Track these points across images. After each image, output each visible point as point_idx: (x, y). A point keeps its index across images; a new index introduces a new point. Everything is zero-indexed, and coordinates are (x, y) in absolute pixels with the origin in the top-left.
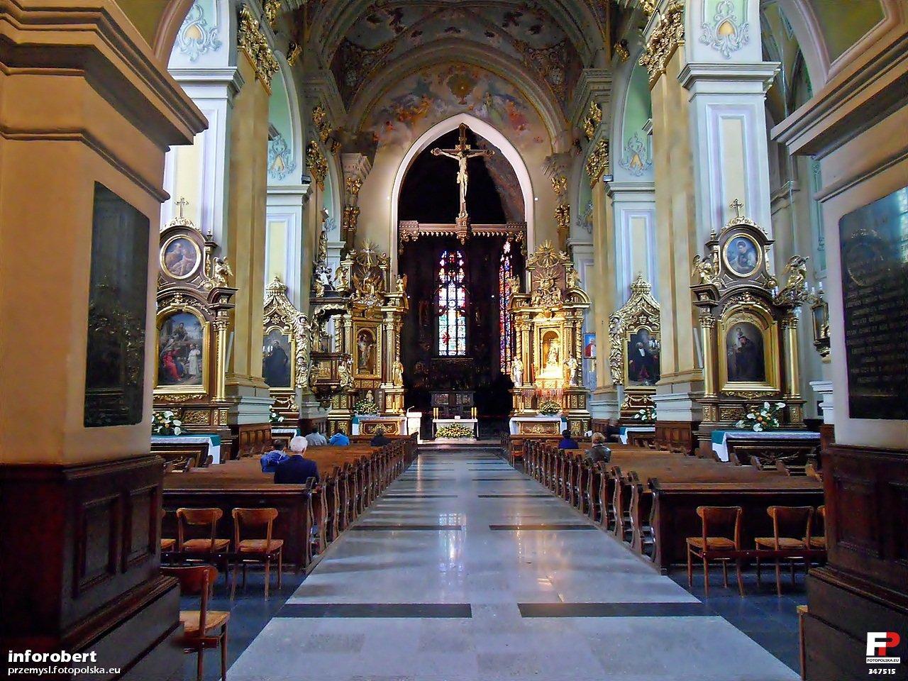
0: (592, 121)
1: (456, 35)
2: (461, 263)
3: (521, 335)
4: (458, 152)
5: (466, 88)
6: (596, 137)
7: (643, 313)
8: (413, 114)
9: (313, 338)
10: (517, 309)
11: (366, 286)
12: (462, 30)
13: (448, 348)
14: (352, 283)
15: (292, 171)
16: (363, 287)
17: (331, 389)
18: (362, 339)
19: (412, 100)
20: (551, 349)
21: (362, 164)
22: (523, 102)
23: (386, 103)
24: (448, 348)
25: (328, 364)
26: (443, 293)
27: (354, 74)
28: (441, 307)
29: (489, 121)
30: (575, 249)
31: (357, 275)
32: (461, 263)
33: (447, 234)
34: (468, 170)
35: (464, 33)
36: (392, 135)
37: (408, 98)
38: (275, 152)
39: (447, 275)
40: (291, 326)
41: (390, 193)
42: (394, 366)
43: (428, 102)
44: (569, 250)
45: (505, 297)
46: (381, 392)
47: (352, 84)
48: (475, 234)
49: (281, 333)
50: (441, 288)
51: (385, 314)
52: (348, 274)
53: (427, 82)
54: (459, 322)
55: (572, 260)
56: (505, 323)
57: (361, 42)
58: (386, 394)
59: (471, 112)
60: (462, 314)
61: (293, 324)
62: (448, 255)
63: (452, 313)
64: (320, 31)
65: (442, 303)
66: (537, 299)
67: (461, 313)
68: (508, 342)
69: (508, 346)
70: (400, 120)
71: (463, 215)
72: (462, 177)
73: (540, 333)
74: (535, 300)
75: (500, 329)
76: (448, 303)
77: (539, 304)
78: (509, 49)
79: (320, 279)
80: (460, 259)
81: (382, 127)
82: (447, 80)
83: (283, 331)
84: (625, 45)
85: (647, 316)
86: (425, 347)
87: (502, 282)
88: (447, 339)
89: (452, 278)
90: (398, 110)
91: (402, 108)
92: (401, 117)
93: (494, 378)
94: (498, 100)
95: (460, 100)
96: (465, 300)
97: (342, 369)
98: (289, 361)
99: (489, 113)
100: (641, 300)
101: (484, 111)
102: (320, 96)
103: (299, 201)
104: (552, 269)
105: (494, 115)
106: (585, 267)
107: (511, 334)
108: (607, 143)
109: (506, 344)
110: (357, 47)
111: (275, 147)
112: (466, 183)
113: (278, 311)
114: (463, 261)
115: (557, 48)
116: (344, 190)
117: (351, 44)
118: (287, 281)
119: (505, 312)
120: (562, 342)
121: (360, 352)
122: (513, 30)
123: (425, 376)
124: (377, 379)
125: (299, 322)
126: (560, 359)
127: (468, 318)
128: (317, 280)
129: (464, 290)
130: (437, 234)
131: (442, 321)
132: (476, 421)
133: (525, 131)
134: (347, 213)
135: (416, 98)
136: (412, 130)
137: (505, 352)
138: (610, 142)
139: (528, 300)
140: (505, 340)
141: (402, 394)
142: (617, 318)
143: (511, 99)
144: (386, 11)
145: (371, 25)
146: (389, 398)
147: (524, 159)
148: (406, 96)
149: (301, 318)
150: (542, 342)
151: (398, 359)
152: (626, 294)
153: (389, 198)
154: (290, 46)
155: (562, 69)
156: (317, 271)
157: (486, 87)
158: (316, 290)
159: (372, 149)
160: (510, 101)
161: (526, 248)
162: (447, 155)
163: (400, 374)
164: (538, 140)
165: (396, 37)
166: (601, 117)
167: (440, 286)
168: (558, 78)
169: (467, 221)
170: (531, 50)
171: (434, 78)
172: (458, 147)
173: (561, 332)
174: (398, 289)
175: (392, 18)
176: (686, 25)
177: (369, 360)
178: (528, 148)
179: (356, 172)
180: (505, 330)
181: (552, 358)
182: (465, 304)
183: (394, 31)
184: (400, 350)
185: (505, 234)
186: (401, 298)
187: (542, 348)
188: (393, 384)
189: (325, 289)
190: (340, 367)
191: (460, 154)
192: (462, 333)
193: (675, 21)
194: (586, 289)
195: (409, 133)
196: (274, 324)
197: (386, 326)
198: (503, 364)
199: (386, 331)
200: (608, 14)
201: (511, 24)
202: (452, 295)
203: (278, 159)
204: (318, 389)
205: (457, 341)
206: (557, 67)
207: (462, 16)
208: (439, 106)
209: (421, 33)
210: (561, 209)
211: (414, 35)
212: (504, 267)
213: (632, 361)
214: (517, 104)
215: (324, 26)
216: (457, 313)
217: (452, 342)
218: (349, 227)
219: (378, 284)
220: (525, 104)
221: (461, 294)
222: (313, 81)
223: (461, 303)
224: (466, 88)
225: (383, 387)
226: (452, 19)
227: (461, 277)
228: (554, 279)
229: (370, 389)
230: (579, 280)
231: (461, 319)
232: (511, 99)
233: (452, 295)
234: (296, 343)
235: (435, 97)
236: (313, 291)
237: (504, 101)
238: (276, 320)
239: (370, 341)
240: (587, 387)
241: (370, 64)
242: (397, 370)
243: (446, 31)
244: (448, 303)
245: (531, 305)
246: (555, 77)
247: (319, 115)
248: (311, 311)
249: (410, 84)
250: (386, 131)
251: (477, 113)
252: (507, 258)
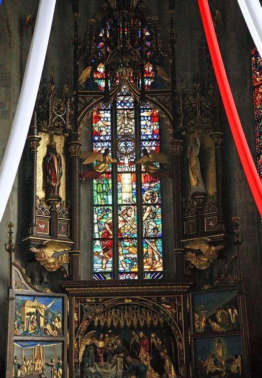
13: (116, 264)
24: (116, 264)
54: (146, 195)
60: (155, 176)
192: (154, 225)
217: (127, 252)
231: (151, 188)
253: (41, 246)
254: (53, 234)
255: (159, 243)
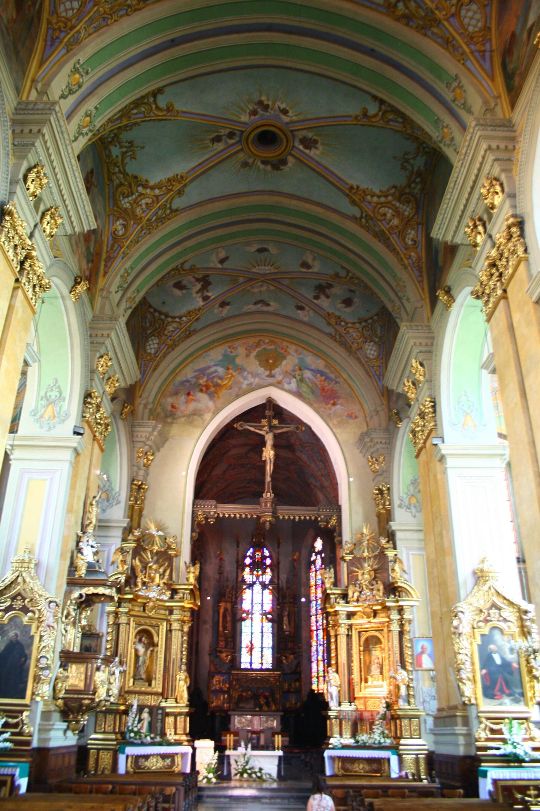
0: (414, 384)
1: (265, 309)
2: (268, 561)
3: (336, 641)
4: (264, 426)
5: (275, 361)
6: (420, 399)
7: (494, 606)
8: (217, 385)
9: (66, 631)
10: (331, 607)
11: (149, 574)
12: (271, 303)
14: (133, 569)
15: (63, 421)
16: (145, 574)
17: (81, 705)
18: (140, 641)
19: (216, 371)
20: (373, 658)
21: (155, 433)
22: (336, 377)
23: (188, 373)
25: (82, 668)
26: (247, 595)
27: (156, 341)
28: (244, 612)
29: (299, 395)
30: (399, 536)
31: (140, 561)
32: (268, 561)
33: (249, 516)
34: (275, 446)
35: (274, 306)
36: (192, 406)
37: (212, 370)
38: (47, 400)
39: (253, 574)
40: (37, 612)
41: (185, 467)
42: (178, 677)
43: (234, 374)
44: (391, 536)
45: (316, 601)
46: (160, 712)
47: (153, 351)
48: (281, 517)
49: (22, 622)
50: (245, 589)
51: (171, 611)
52: (129, 558)
53: (234, 354)
55: (395, 548)
56: (317, 630)
57: (164, 310)
58: (168, 714)
59: (279, 385)
60: (270, 620)
61: (39, 610)
62: (254, 553)
63: (257, 617)
64: (117, 281)
65: (246, 606)
66: (356, 594)
67: (267, 618)
68: (321, 654)
69: (320, 658)
70: (201, 391)
71: (268, 495)
72: (269, 453)
73: (360, 637)
74: (353, 597)
75: (311, 638)
76: (252, 607)
77: (358, 601)
78: (321, 323)
79: (82, 554)
80: (268, 557)
81: (183, 398)
82: (255, 353)
83: (25, 619)
84: (448, 292)
85: (499, 609)
86: (226, 657)
87: (313, 582)
88: (251, 649)
89: (258, 577)
90: (201, 381)
91: (205, 379)
92: (204, 388)
93: (305, 699)
94: (308, 374)
95: (268, 373)
96: (273, 604)
97: (100, 677)
98: (28, 661)
99: (298, 386)
100: (490, 588)
101: (293, 385)
102: (108, 342)
103: (68, 455)
104: (372, 559)
105: (304, 389)
106: (411, 557)
107: (324, 644)
108: (434, 402)
109: (317, 655)
110: (161, 313)
111: (48, 394)
112: (272, 460)
113: (23, 592)
114: (271, 559)
115: (370, 321)
116: (132, 464)
117: (156, 311)
118: (39, 554)
119: (316, 618)
120: (386, 648)
121: (137, 656)
122: (324, 303)
123: (224, 692)
124: (156, 694)
125: (47, 607)
126: (386, 674)
127: (276, 625)
128: (79, 555)
129: (272, 593)
130: (238, 516)
131: (245, 626)
132: (280, 753)
133: (338, 407)
134: (134, 487)
135: (221, 370)
136: (215, 402)
137: (318, 665)
138: (437, 402)
139: (345, 596)
140: (317, 651)
141: (187, 714)
142: (462, 612)
143: (322, 373)
144: (194, 277)
145: (177, 292)
146: (170, 720)
147: (338, 436)
148: (210, 367)
149: (51, 602)
150: (362, 648)
151: (184, 667)
152: (470, 581)
153: (184, 473)
154: (76, 279)
155: (375, 343)
156: (81, 544)
157: (296, 361)
158: (76, 567)
159: (169, 420)
160: (321, 376)
161: (340, 535)
162: (252, 429)
163: (185, 688)
164: (351, 416)
165: (203, 306)
166: (424, 376)
167: (245, 587)
168: (372, 352)
169: (272, 503)
170: (343, 323)
171: (241, 351)
172: (264, 422)
173: (386, 635)
174: (188, 579)
175: (199, 286)
176: (526, 239)
177: (147, 668)
178: (341, 424)
179: (149, 443)
180: (317, 640)
181: (375, 670)
182: (272, 608)
183: (201, 300)
184: (187, 656)
185: (316, 518)
186: (191, 590)
187: (362, 657)
188: (177, 702)
189: (88, 567)
190: (97, 674)
191: (266, 428)
192: (269, 641)
193: (515, 236)
194: (413, 580)
195: (211, 404)
196: (14, 609)
197: (171, 625)
198: (314, 680)
199: (171, 631)
200: (425, 275)
201: (323, 297)
202: (257, 598)
203: (50, 408)
204: (65, 704)
205: (262, 651)
206: (371, 341)
207: (272, 288)
208: (245, 378)
209: (228, 304)
210: (379, 490)
211: (223, 304)
212: (315, 567)
213: (484, 671)
214: (327, 378)
215: (121, 276)
216: (262, 618)
217: (256, 652)
218: (136, 503)
219: (165, 571)
220: (338, 380)
221: (268, 597)
222: (101, 326)
223: (268, 607)
224: (275, 361)
225: (163, 704)
226: (261, 291)
227: (267, 577)
228: (375, 570)
229: (147, 706)
230: (404, 571)
231: (268, 626)
232: (322, 373)
233: (257, 598)
234: (41, 637)
235: (241, 369)
236: (73, 567)
237: (315, 377)
238: (18, 604)
239: (151, 644)
240: (421, 708)
241: (173, 331)
242: (182, 683)
243: (256, 303)
244: (252, 607)
245: (347, 603)
246: (368, 352)
247: (102, 366)
248: (68, 594)
249: (217, 354)
250: (187, 402)
251: (286, 386)
252: (319, 556)
253: (221, 652)
254: (226, 647)
255: (271, 650)
